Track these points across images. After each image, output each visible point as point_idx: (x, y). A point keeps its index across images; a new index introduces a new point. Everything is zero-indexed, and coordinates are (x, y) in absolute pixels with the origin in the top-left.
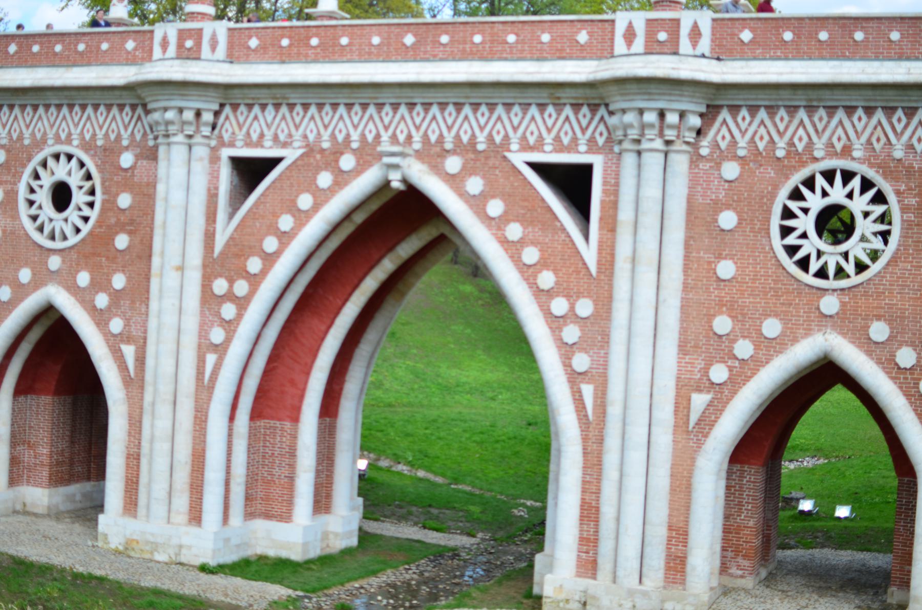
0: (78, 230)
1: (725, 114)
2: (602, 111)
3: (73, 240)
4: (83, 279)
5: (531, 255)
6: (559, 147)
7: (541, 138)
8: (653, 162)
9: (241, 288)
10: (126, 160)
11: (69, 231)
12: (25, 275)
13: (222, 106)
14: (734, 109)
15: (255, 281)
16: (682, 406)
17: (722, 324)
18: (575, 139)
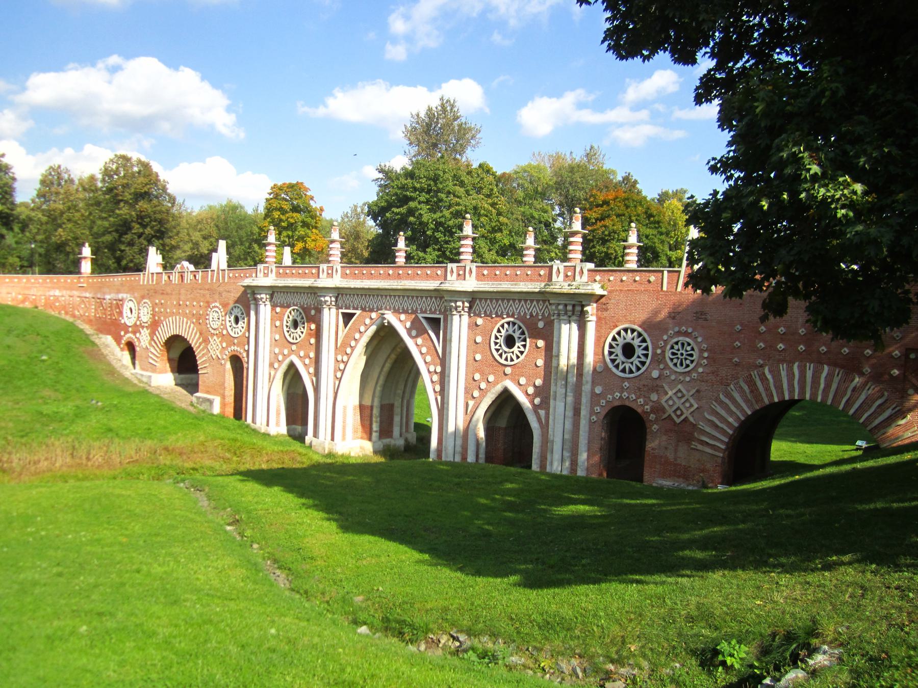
0: (300, 337)
1: (478, 301)
2: (443, 300)
3: (299, 340)
4: (302, 354)
5: (424, 350)
6: (431, 313)
7: (426, 309)
8: (456, 318)
9: (345, 358)
10: (313, 312)
11: (298, 337)
12: (286, 352)
13: (338, 294)
14: (481, 300)
15: (349, 356)
16: (467, 405)
17: (477, 376)
18: (435, 309)
